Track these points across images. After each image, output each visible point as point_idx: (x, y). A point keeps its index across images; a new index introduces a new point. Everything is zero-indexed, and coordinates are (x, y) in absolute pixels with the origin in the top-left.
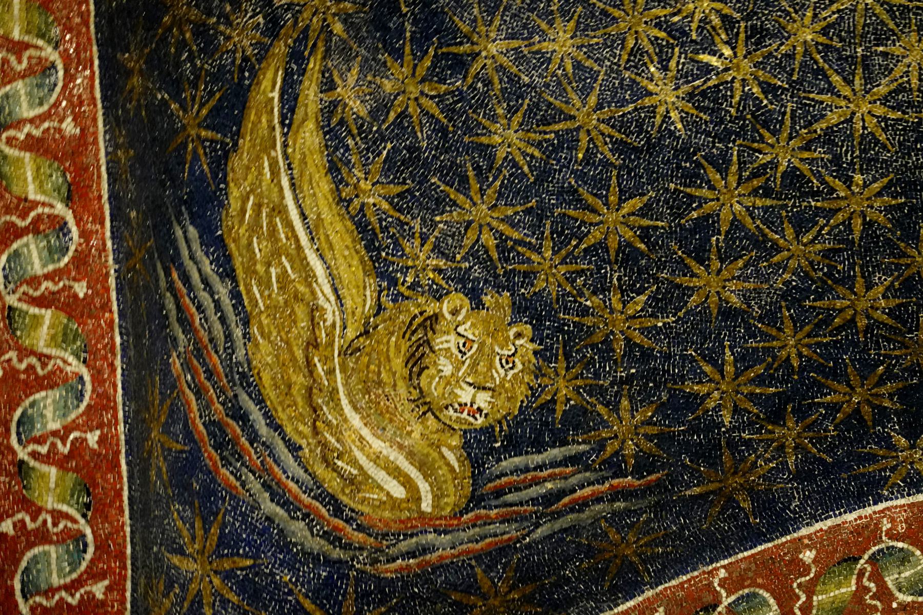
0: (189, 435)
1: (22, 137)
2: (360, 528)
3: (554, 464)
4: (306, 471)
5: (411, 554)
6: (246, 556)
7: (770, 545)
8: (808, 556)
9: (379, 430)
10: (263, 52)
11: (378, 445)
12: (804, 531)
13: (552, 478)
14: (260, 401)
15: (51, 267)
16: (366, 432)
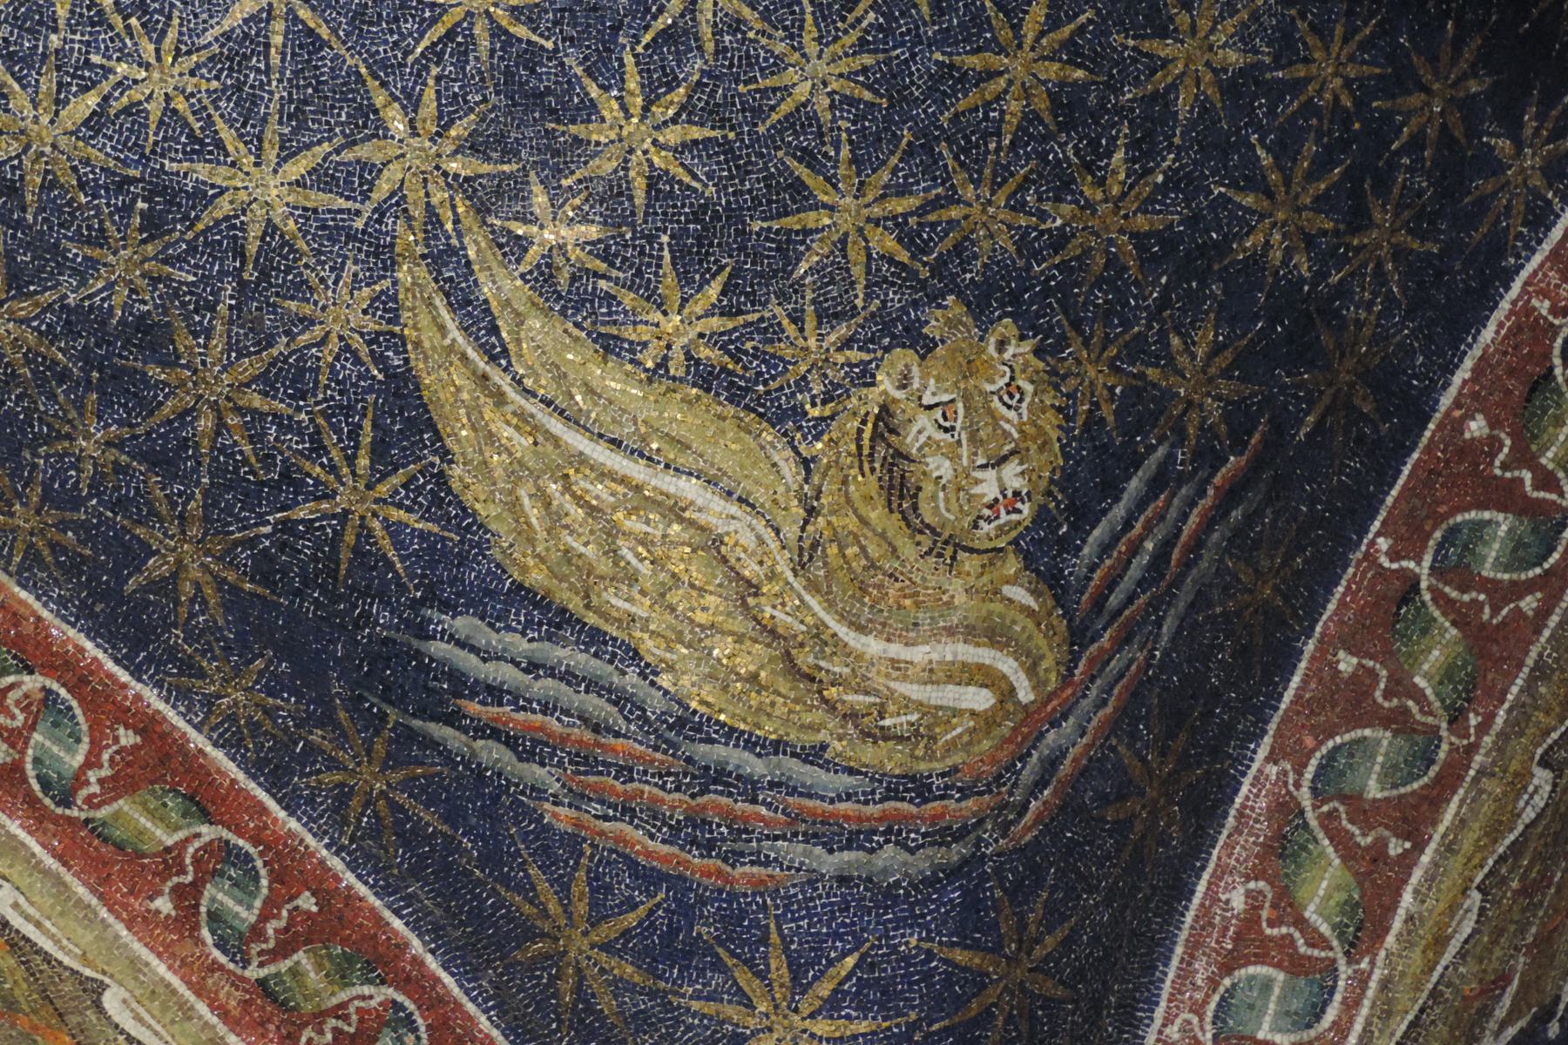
0: (649, 878)
1: (95, 789)
2: (965, 793)
3: (1141, 504)
4: (851, 771)
5: (1041, 784)
6: (844, 954)
7: (1415, 456)
8: (1477, 427)
9: (909, 632)
10: (388, 306)
11: (919, 654)
12: (1446, 401)
13: (1148, 529)
14: (730, 733)
15: (258, 903)
16: (896, 650)
